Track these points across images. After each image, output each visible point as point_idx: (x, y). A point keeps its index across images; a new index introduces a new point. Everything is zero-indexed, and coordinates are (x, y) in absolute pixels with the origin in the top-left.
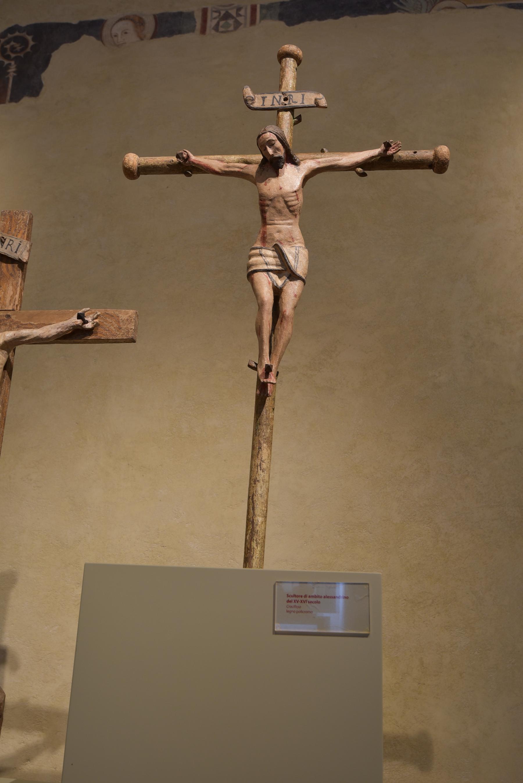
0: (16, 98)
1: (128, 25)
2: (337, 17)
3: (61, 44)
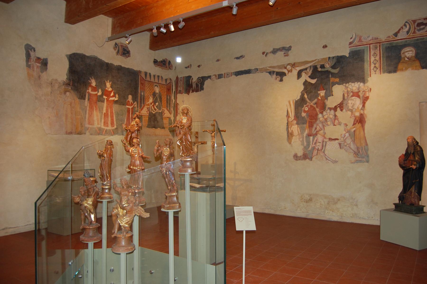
0: (201, 91)
1: (214, 76)
2: (243, 75)
3: (205, 80)
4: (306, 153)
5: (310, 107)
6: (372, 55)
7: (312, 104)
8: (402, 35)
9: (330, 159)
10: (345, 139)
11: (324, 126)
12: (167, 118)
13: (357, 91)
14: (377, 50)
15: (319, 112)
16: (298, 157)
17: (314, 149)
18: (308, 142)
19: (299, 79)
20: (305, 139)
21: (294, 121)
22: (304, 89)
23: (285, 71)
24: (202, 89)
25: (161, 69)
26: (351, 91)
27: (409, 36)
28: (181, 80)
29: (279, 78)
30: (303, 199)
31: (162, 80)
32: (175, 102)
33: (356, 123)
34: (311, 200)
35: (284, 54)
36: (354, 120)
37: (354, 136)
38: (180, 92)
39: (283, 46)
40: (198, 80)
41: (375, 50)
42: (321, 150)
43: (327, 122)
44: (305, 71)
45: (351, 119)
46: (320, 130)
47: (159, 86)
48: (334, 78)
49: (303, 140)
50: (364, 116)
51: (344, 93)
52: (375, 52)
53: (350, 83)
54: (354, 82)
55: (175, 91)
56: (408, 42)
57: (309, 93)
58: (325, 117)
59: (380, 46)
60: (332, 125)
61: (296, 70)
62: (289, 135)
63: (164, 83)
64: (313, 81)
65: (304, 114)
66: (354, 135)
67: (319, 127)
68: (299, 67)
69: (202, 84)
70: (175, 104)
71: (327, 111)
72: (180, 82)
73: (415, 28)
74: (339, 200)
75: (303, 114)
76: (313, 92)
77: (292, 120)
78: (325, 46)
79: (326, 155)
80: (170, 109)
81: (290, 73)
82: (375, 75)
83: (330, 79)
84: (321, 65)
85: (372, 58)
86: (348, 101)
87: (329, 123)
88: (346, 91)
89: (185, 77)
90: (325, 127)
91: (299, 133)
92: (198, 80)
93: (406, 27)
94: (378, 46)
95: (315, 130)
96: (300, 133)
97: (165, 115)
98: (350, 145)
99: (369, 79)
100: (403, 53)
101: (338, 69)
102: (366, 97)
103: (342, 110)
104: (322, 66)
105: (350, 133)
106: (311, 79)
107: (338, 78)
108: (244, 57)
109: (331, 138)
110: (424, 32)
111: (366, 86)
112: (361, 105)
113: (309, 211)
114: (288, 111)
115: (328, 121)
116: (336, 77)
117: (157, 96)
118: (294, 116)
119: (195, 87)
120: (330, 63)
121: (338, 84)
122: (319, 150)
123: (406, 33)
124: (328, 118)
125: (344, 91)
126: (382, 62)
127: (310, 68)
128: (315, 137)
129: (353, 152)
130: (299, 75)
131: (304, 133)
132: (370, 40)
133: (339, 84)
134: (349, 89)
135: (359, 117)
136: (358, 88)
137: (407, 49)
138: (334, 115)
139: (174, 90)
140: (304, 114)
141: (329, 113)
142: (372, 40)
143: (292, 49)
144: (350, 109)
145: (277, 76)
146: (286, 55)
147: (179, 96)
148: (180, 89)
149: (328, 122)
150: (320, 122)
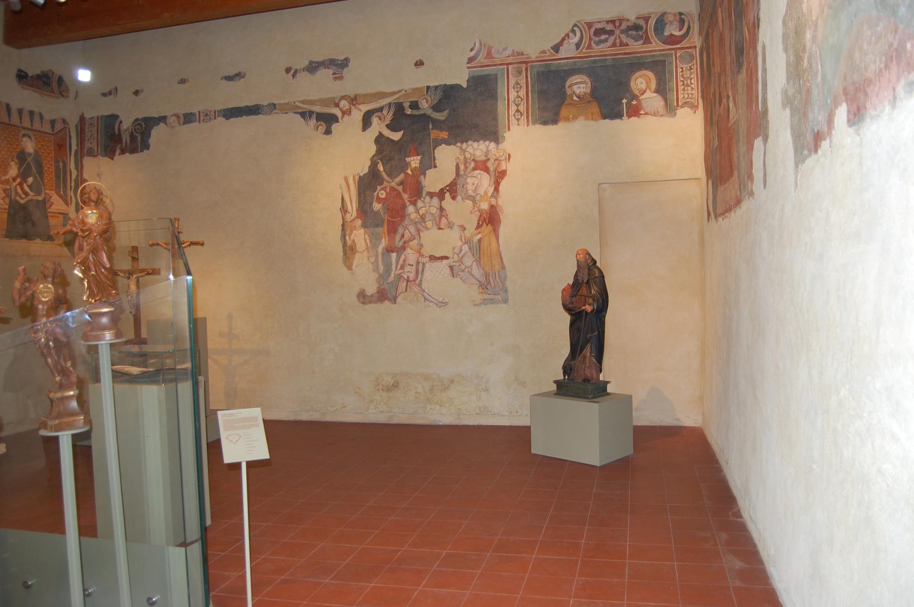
0: (142, 151)
1: (174, 118)
2: (241, 117)
4: (383, 287)
5: (390, 191)
6: (513, 85)
7: (393, 184)
8: (569, 50)
9: (432, 300)
10: (460, 257)
11: (418, 231)
12: (57, 215)
13: (483, 158)
14: (522, 76)
15: (409, 201)
16: (367, 296)
17: (400, 278)
18: (388, 265)
19: (367, 131)
20: (380, 259)
21: (356, 219)
22: (376, 151)
23: (337, 112)
24: (146, 146)
25: (37, 95)
26: (472, 158)
27: (579, 53)
28: (91, 124)
29: (323, 128)
30: (381, 386)
31: (42, 123)
32: (77, 176)
33: (482, 224)
34: (396, 385)
35: (333, 74)
36: (477, 219)
37: (478, 250)
38: (91, 153)
39: (332, 57)
40: (136, 126)
41: (517, 77)
42: (414, 281)
43: (425, 222)
44: (379, 114)
45: (472, 215)
46: (411, 240)
47: (33, 137)
48: (437, 131)
49: (376, 261)
50: (498, 209)
51: (458, 161)
52: (517, 80)
53: (470, 142)
54: (478, 141)
55: (76, 151)
56: (579, 64)
57: (387, 161)
58: (421, 212)
59: (526, 69)
60: (435, 228)
61: (361, 111)
62: (346, 250)
63: (47, 128)
64: (396, 136)
65: (377, 206)
66: (478, 248)
67: (409, 231)
68: (364, 104)
69: (146, 135)
70: (78, 180)
71: (424, 199)
72: (91, 128)
73: (590, 39)
74: (453, 381)
75: (376, 206)
76: (396, 157)
77: (352, 218)
78: (418, 63)
79: (424, 291)
80: (65, 192)
81: (346, 117)
82: (517, 126)
83: (429, 132)
84: (411, 102)
85: (511, 92)
86: (466, 179)
87: (429, 224)
88: (462, 158)
89: (101, 116)
90: (420, 232)
91: (368, 246)
92: (134, 125)
93: (575, 35)
94: (524, 69)
95: (401, 239)
96: (369, 246)
97: (53, 207)
98: (471, 269)
99: (507, 135)
100: (569, 87)
101: (446, 113)
102: (501, 171)
103: (454, 198)
104: (414, 105)
105: (472, 245)
106: (392, 131)
107: (446, 131)
108: (244, 77)
109: (434, 256)
110: (606, 48)
111: (501, 149)
112: (492, 187)
113: (393, 410)
114: (343, 199)
115: (427, 219)
116: (441, 129)
117: (29, 164)
118: (357, 210)
119: (128, 141)
120: (429, 99)
121: (445, 144)
122: (411, 281)
123: (574, 47)
124: (427, 215)
125: (458, 157)
126: (530, 103)
127: (390, 107)
128: (402, 254)
129: (477, 284)
130: (366, 122)
131: (377, 247)
132: (508, 57)
133: (448, 143)
134: (468, 156)
135: (488, 212)
136: (486, 152)
137: (576, 79)
138: (438, 207)
139: (74, 148)
140: (377, 206)
141: (428, 205)
142: (512, 56)
143: (351, 64)
144: (471, 196)
145: (319, 123)
146: (338, 77)
147: (88, 162)
148: (90, 145)
149: (427, 223)
150: (411, 223)
